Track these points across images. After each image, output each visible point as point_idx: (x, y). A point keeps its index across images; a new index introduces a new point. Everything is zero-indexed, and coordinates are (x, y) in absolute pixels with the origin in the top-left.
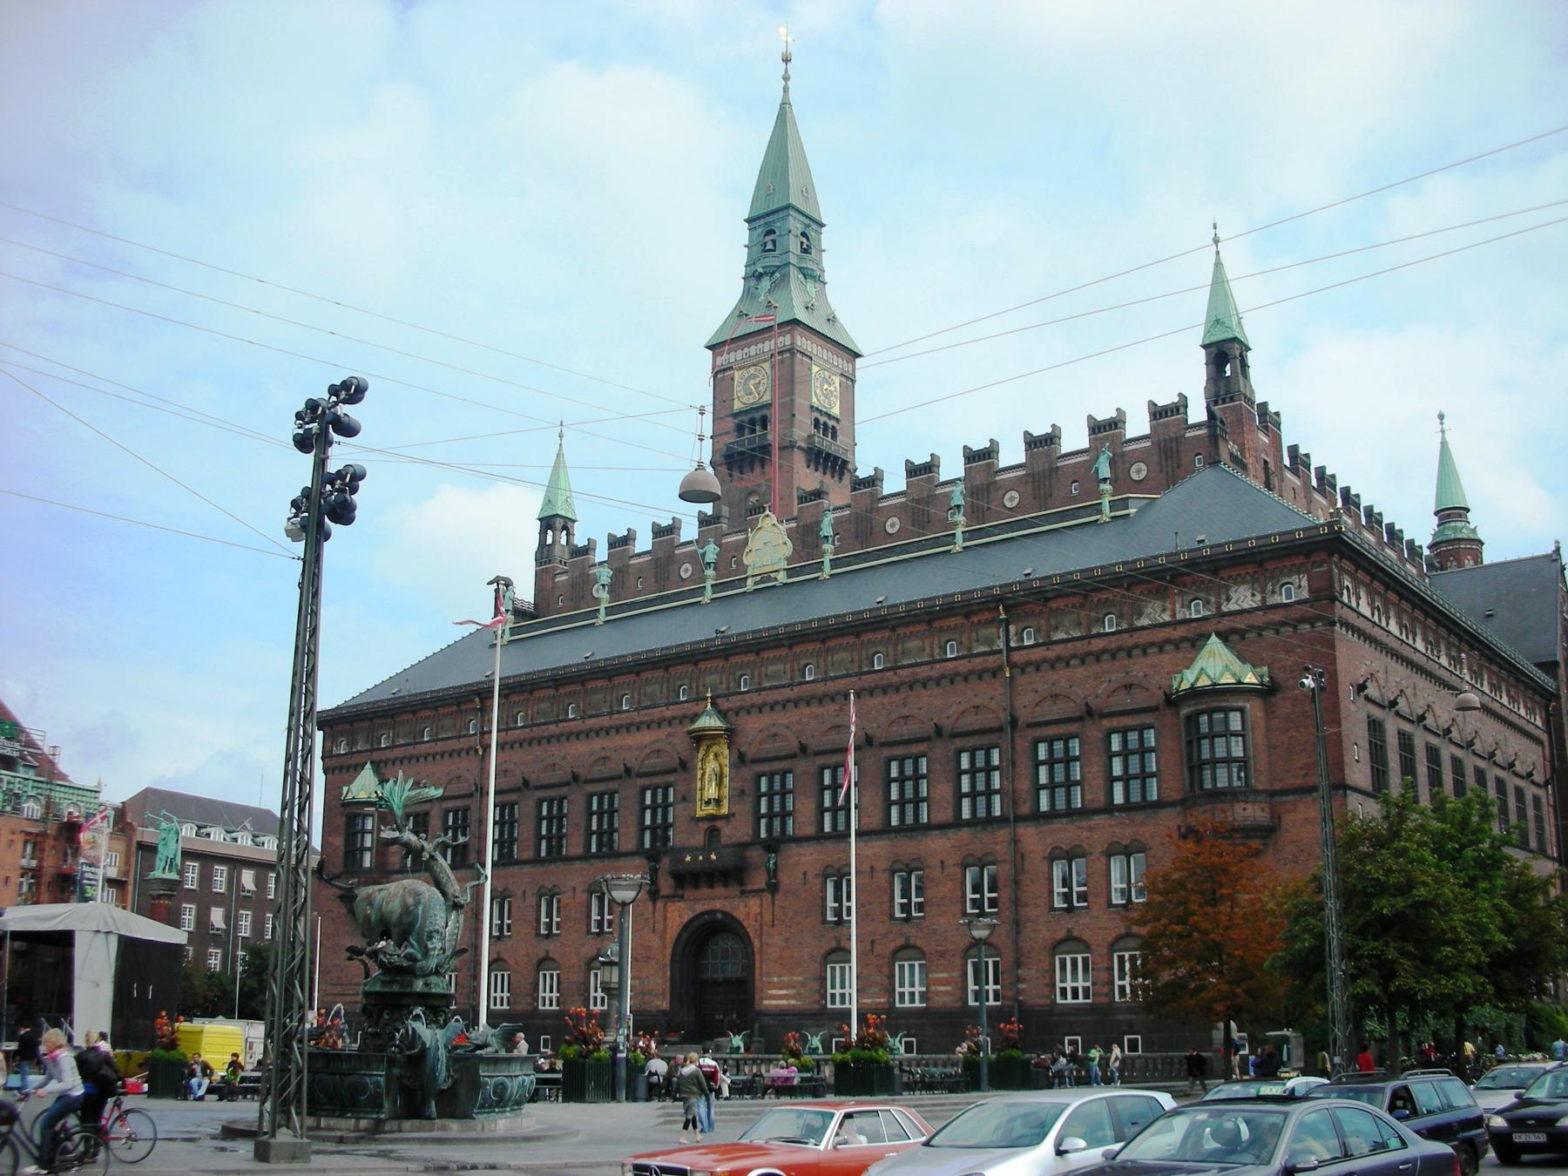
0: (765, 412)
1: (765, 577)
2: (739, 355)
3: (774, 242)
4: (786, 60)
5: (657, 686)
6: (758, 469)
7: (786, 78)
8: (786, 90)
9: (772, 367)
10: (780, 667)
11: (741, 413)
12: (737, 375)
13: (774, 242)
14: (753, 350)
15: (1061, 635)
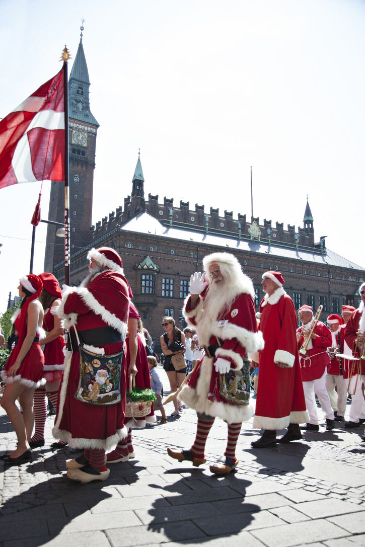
0: (84, 150)
1: (255, 238)
2: (75, 125)
3: (82, 92)
4: (82, 29)
5: (255, 262)
6: (80, 167)
7: (81, 35)
8: (81, 39)
9: (88, 136)
10: (286, 267)
11: (75, 145)
12: (74, 132)
13: (82, 92)
14: (80, 127)
15: (337, 278)
